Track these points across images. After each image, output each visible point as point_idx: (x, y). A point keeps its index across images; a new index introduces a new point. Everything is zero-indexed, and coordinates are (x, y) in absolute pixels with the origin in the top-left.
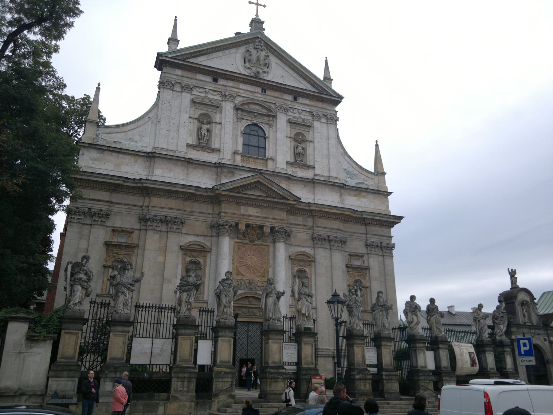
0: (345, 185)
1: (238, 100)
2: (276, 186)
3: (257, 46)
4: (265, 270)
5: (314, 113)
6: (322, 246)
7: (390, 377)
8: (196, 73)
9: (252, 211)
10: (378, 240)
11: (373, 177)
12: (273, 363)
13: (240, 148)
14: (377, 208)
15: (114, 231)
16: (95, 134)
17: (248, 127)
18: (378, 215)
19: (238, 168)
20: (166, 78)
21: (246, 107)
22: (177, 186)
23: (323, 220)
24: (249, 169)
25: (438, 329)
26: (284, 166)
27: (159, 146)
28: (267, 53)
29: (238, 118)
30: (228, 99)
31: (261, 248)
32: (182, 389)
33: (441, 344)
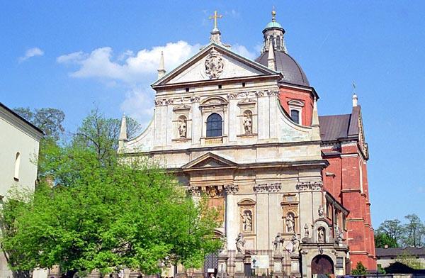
5: (257, 92)
9: (209, 178)
13: (205, 135)
26: (235, 139)
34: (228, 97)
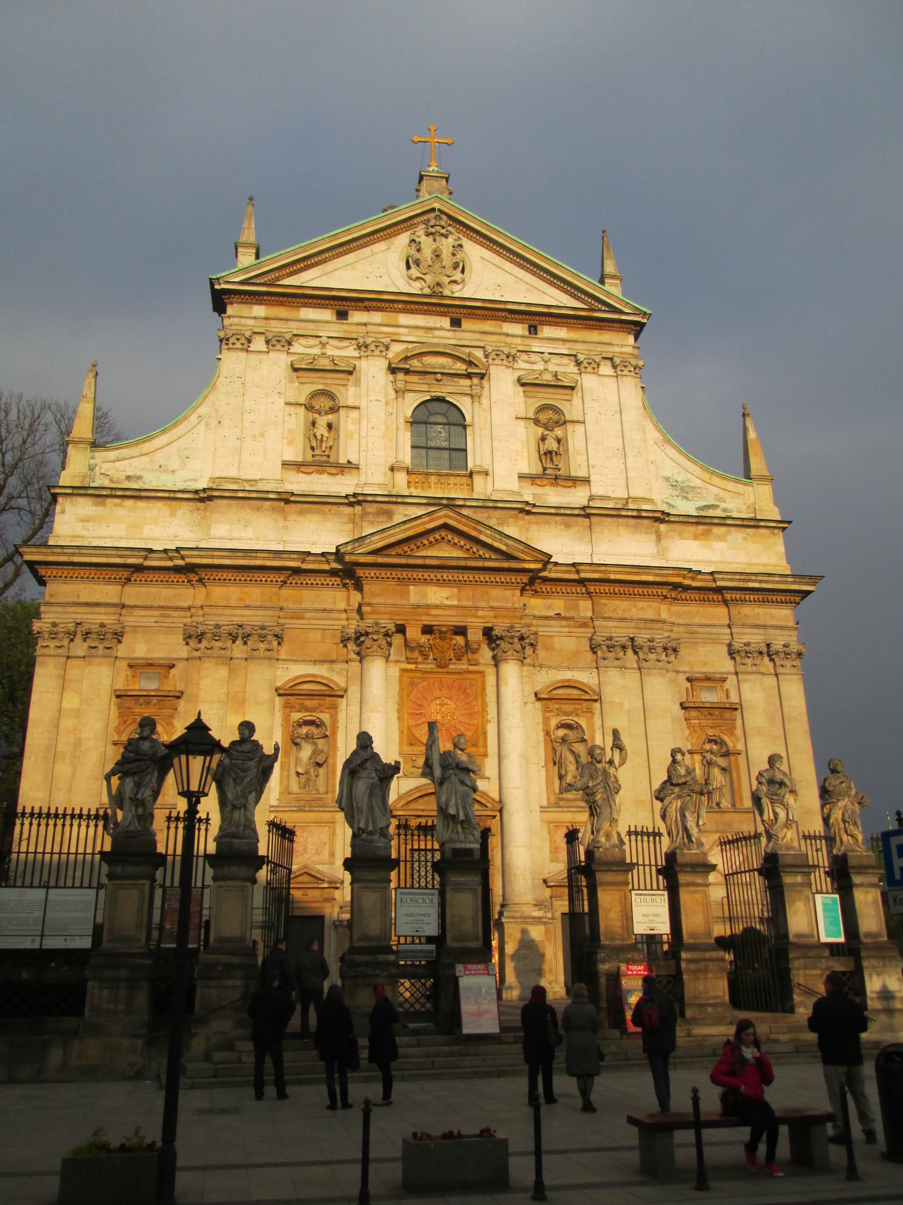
0: (668, 514)
1: (396, 349)
2: (489, 532)
3: (432, 227)
4: (477, 730)
5: (581, 357)
6: (618, 663)
7: (702, 964)
8: (299, 307)
9: (436, 595)
10: (762, 637)
11: (741, 488)
12: (366, 938)
13: (406, 456)
14: (755, 561)
15: (137, 666)
16: (87, 468)
17: (423, 407)
18: (753, 578)
19: (399, 500)
20: (233, 327)
21: (415, 364)
22: (259, 555)
23: (618, 602)
24: (424, 501)
25: (852, 836)
26: (514, 485)
27: (223, 475)
28: (459, 239)
29: (396, 392)
30: (372, 351)
31: (466, 679)
32: (111, 1006)
33: (858, 873)
34: (487, 356)
